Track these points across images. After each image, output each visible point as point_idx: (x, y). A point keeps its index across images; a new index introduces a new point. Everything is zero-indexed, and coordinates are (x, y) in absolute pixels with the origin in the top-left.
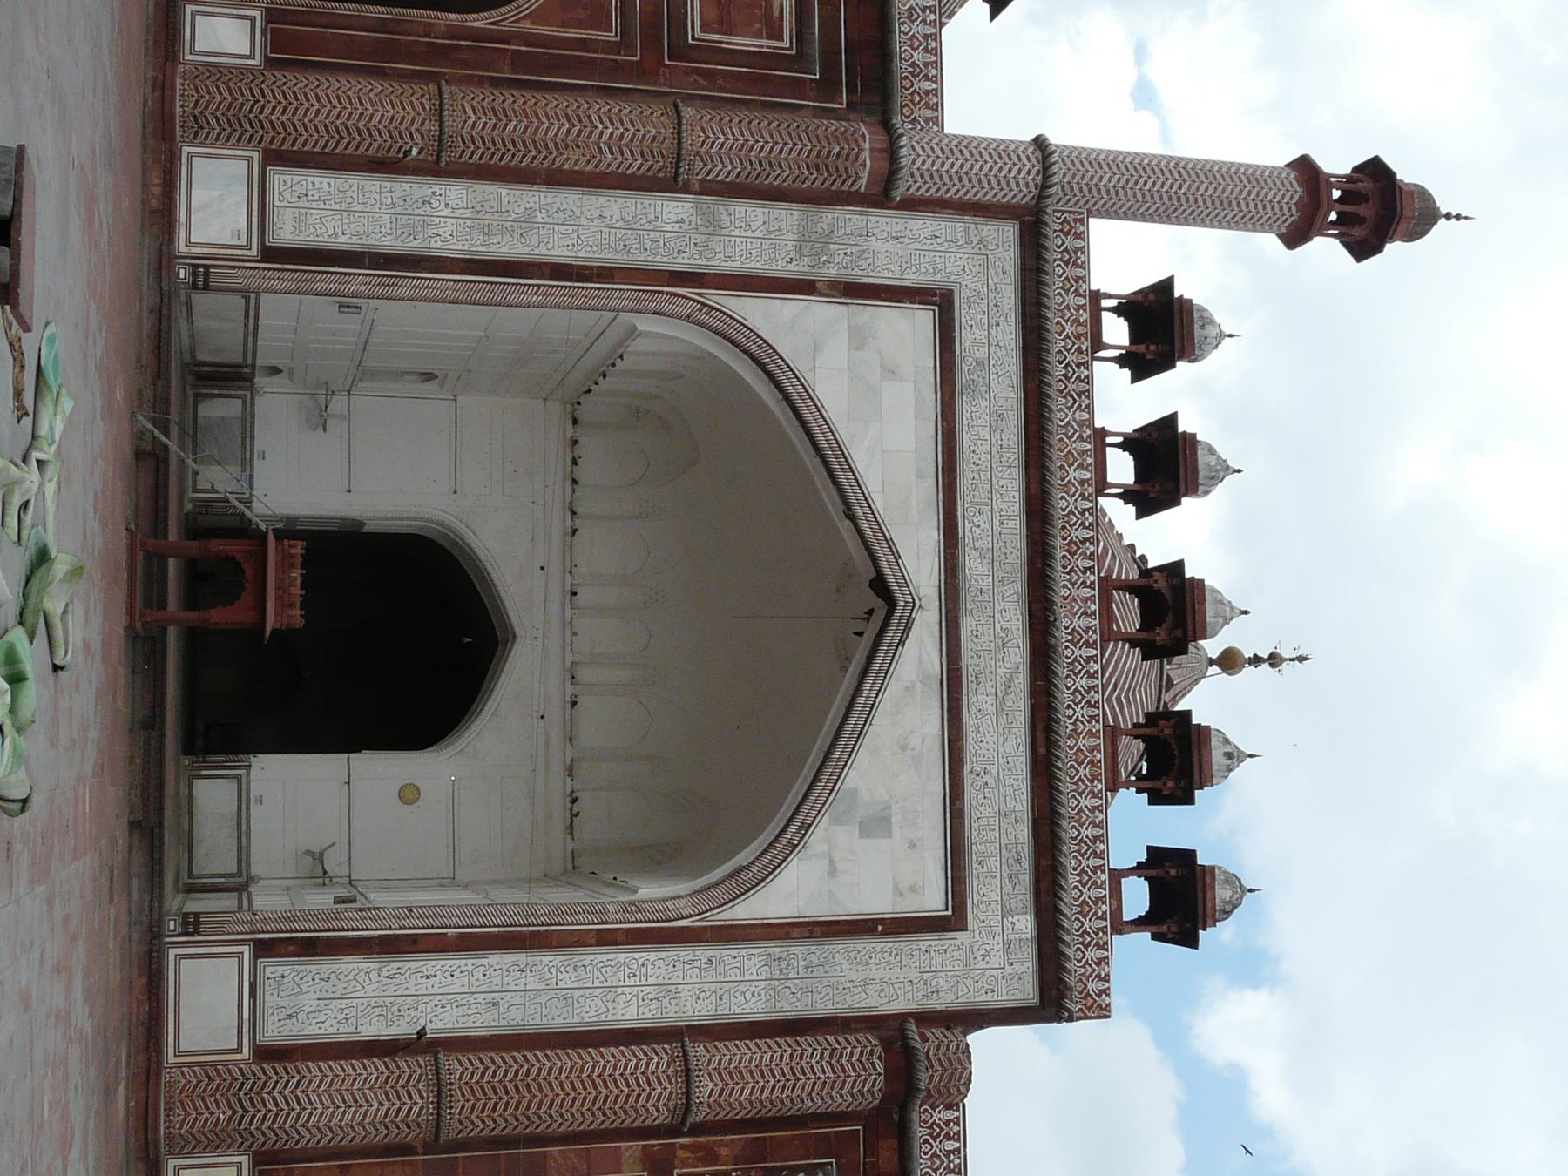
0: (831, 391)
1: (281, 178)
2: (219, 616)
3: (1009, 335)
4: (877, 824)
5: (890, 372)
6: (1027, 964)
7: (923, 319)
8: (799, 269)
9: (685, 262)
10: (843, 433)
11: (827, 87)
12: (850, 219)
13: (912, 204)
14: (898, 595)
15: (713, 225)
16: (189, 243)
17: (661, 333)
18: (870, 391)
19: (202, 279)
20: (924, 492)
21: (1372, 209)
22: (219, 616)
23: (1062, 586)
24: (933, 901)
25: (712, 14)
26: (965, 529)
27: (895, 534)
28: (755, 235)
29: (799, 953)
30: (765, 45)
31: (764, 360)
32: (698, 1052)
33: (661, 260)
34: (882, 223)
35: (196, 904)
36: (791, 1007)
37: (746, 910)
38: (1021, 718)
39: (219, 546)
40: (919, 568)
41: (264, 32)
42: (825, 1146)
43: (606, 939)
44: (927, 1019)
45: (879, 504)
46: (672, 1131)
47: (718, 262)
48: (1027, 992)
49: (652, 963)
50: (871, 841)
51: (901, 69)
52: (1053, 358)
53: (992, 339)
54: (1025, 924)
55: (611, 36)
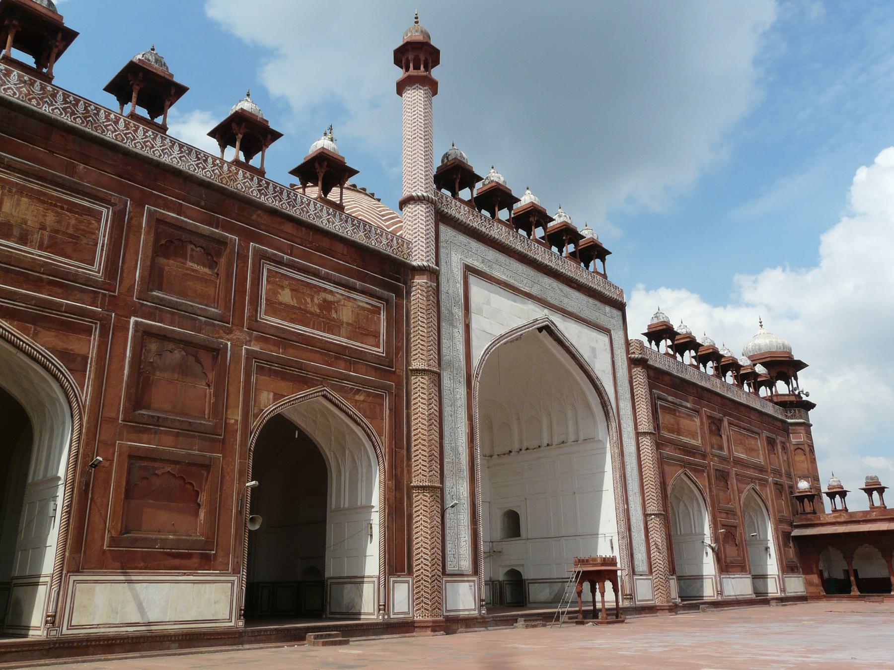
5: (488, 302)
11: (398, 292)
14: (544, 324)
16: (474, 610)
19: (481, 603)
25: (371, 340)
27: (531, 320)
41: (399, 576)
54: (608, 309)
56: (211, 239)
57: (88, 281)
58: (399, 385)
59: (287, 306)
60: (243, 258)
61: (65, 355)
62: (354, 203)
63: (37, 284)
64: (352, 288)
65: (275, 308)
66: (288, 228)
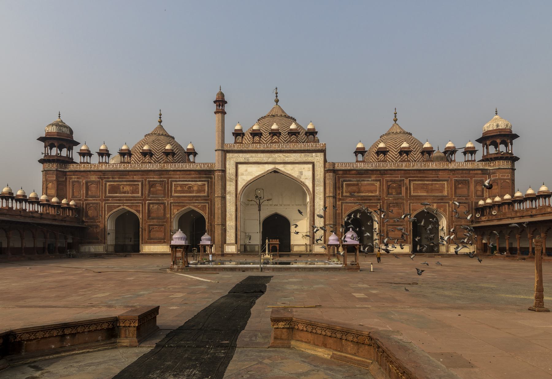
0: (249, 178)
1: (227, 242)
2: (278, 248)
3: (241, 155)
4: (301, 173)
5: (246, 171)
6: (319, 154)
7: (239, 166)
8: (234, 182)
9: (234, 196)
10: (254, 177)
11: (211, 178)
12: (228, 175)
13: (225, 167)
15: (229, 192)
17: (241, 199)
18: (249, 173)
19: (238, 250)
20: (261, 166)
21: (221, 102)
22: (278, 248)
23: (272, 149)
24: (310, 166)
26: (266, 161)
28: (230, 187)
29: (316, 183)
30: (206, 186)
31: (246, 186)
32: (327, 195)
33: (234, 199)
34: (228, 171)
35: (308, 250)
36: (322, 184)
37: (311, 190)
38: (289, 154)
39: (271, 248)
40: (270, 167)
42: (339, 180)
43: (314, 206)
44: (325, 167)
45: (263, 172)
46: (336, 198)
47: (234, 192)
48: (322, 154)
49: (317, 200)
50: (303, 174)
51: (208, 169)
52: (243, 149)
53: (241, 157)
54: (314, 154)
55: (207, 205)
56: (160, 181)
57: (138, 197)
58: (211, 201)
59: (179, 190)
60: (168, 183)
61: (137, 211)
62: (198, 159)
63: (131, 200)
64: (196, 181)
65: (176, 192)
66: (178, 173)
